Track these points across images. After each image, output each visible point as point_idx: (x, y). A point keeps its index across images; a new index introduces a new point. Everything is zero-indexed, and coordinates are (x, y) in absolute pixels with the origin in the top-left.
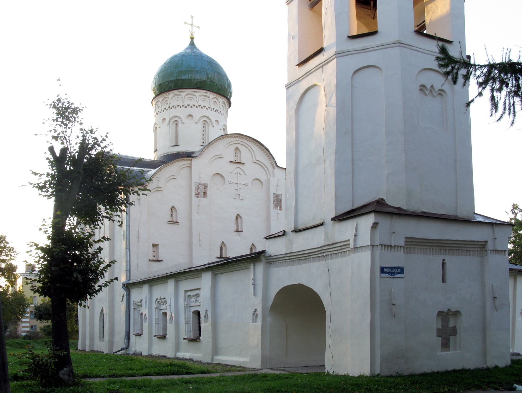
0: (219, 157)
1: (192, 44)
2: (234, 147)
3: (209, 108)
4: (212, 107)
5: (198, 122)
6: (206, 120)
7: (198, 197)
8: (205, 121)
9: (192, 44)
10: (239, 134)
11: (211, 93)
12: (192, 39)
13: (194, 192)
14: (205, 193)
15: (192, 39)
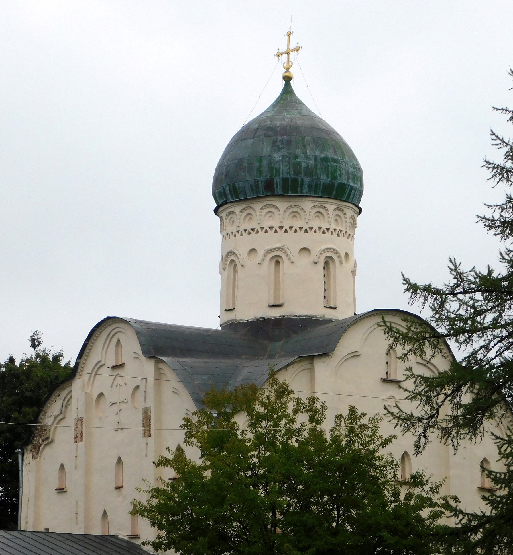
0: (100, 365)
1: (288, 90)
2: (115, 340)
3: (238, 232)
4: (241, 230)
5: (226, 268)
6: (233, 257)
7: (76, 442)
8: (233, 261)
9: (288, 90)
10: (108, 318)
11: (235, 204)
12: (288, 79)
13: (73, 437)
14: (82, 433)
15: (288, 79)
